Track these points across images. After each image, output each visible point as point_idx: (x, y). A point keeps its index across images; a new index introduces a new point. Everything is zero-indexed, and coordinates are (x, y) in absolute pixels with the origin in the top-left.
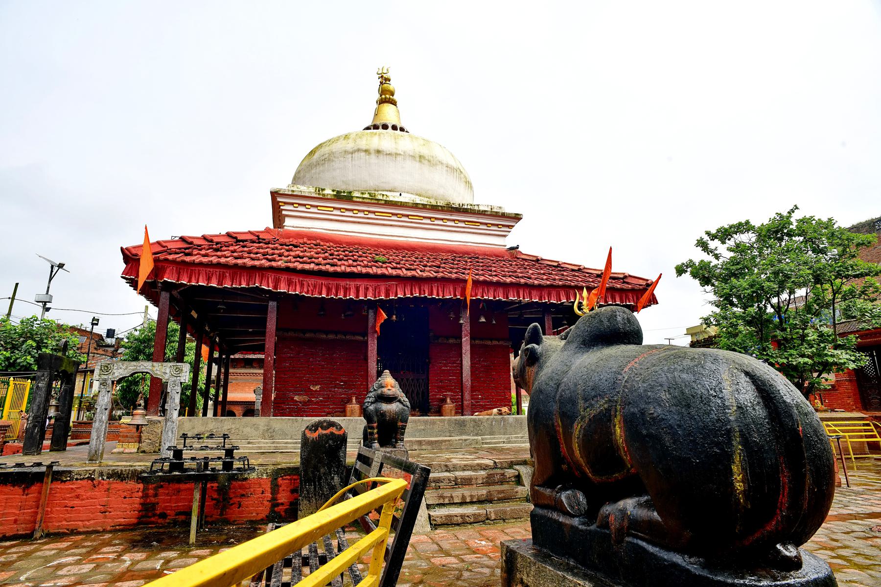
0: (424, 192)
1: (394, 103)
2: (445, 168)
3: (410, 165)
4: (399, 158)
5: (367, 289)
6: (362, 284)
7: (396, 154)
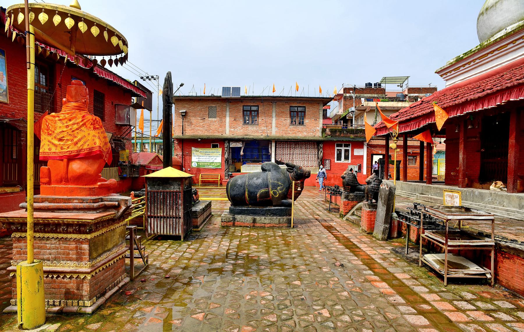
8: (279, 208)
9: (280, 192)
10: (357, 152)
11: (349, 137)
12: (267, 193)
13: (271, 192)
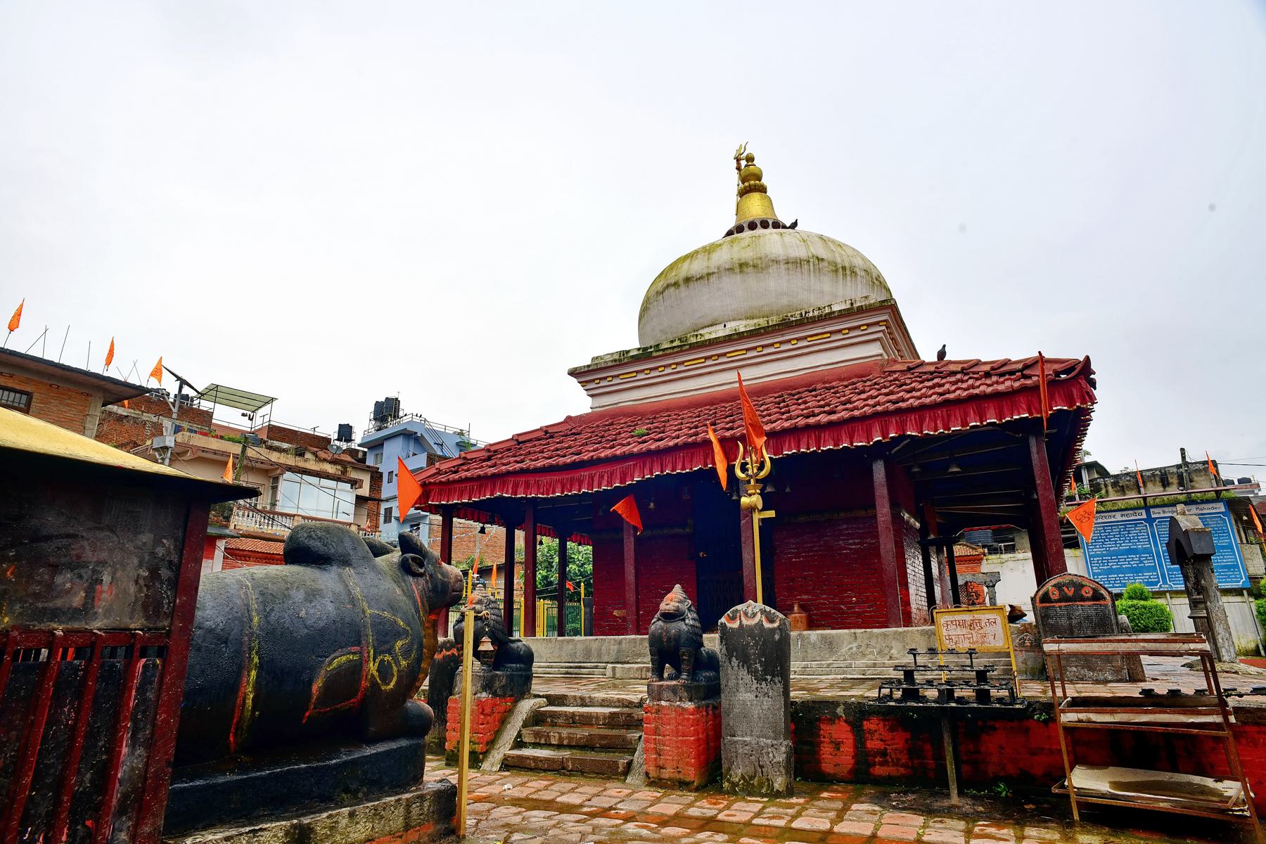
0: (756, 312)
2: (783, 267)
3: (728, 282)
4: (713, 279)
5: (602, 477)
7: (709, 274)
8: (394, 745)
9: (404, 663)
12: (355, 670)
13: (373, 667)
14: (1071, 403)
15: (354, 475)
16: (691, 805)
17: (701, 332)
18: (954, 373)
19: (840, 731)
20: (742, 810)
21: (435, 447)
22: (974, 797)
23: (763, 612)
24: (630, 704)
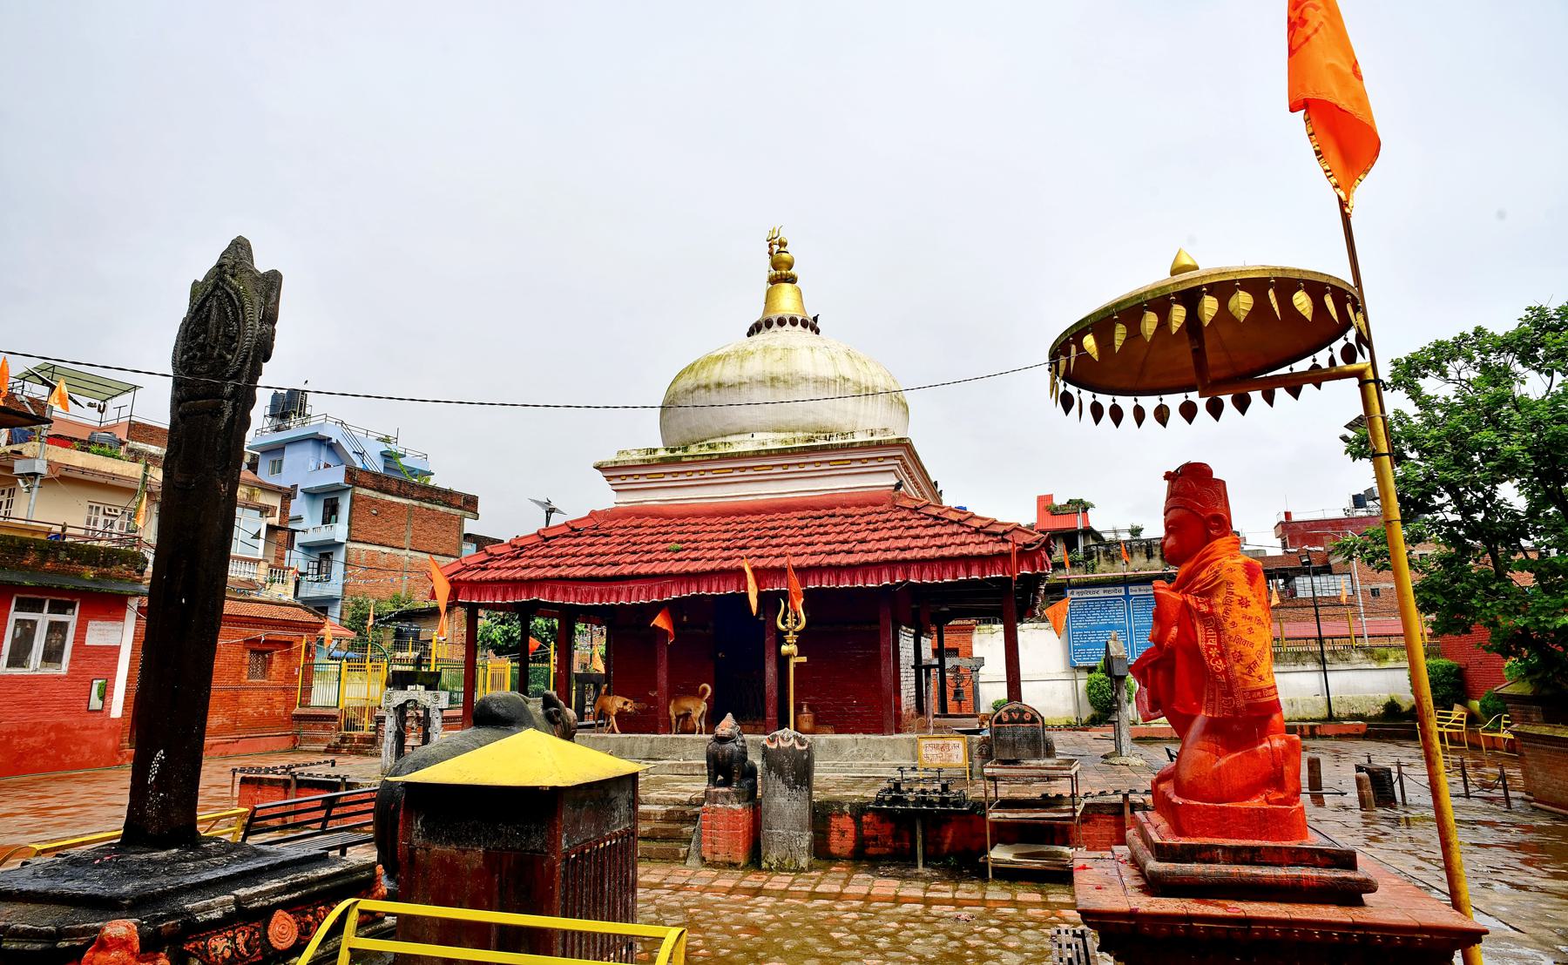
1: (792, 280)
2: (812, 385)
5: (640, 591)
6: (635, 586)
10: (99, 634)
11: (78, 575)
14: (1034, 569)
15: (264, 499)
16: (742, 879)
17: (728, 439)
18: (952, 522)
19: (847, 823)
20: (780, 882)
21: (354, 457)
22: (933, 867)
23: (796, 737)
24: (681, 803)
